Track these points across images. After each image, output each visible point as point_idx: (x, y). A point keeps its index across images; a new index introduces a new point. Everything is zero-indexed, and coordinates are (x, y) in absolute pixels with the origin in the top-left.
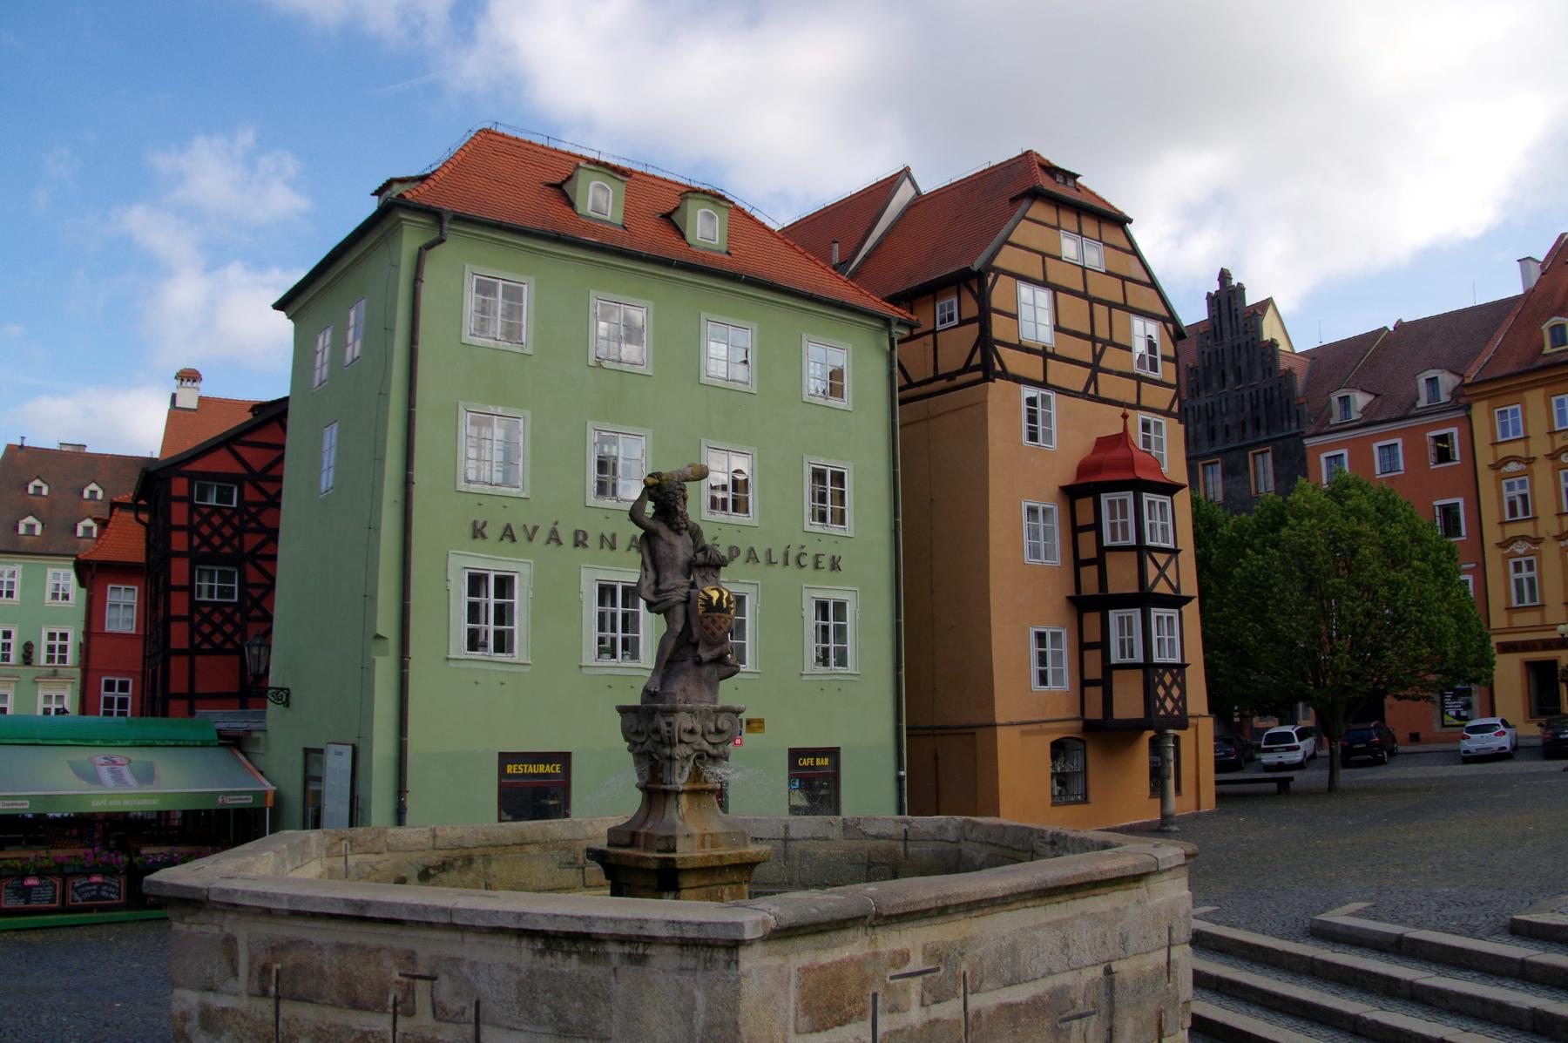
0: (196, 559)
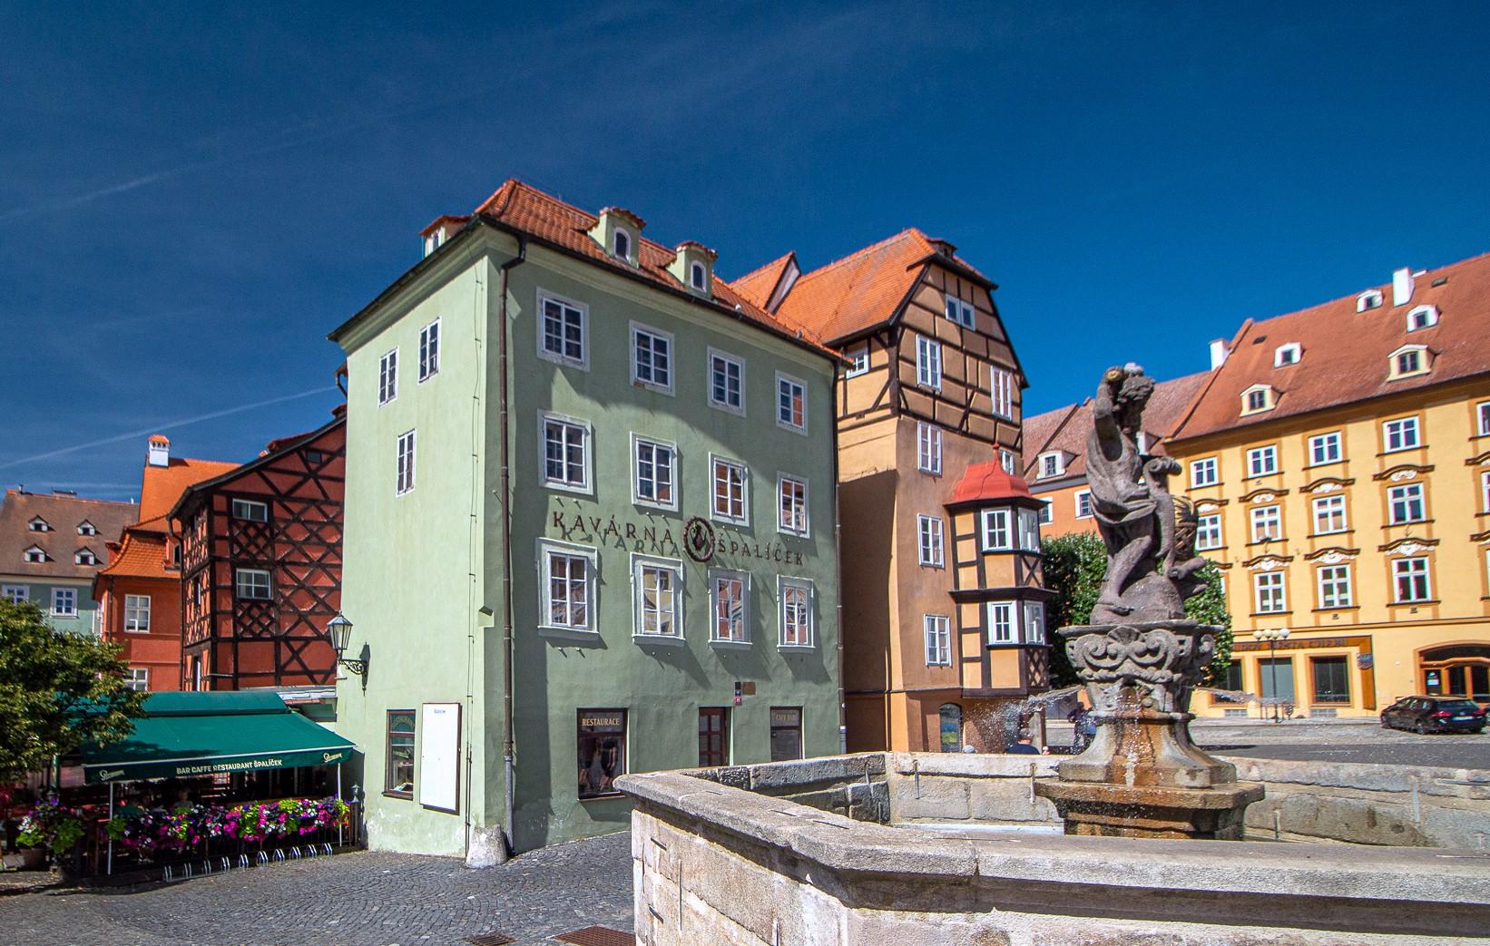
0: (236, 563)
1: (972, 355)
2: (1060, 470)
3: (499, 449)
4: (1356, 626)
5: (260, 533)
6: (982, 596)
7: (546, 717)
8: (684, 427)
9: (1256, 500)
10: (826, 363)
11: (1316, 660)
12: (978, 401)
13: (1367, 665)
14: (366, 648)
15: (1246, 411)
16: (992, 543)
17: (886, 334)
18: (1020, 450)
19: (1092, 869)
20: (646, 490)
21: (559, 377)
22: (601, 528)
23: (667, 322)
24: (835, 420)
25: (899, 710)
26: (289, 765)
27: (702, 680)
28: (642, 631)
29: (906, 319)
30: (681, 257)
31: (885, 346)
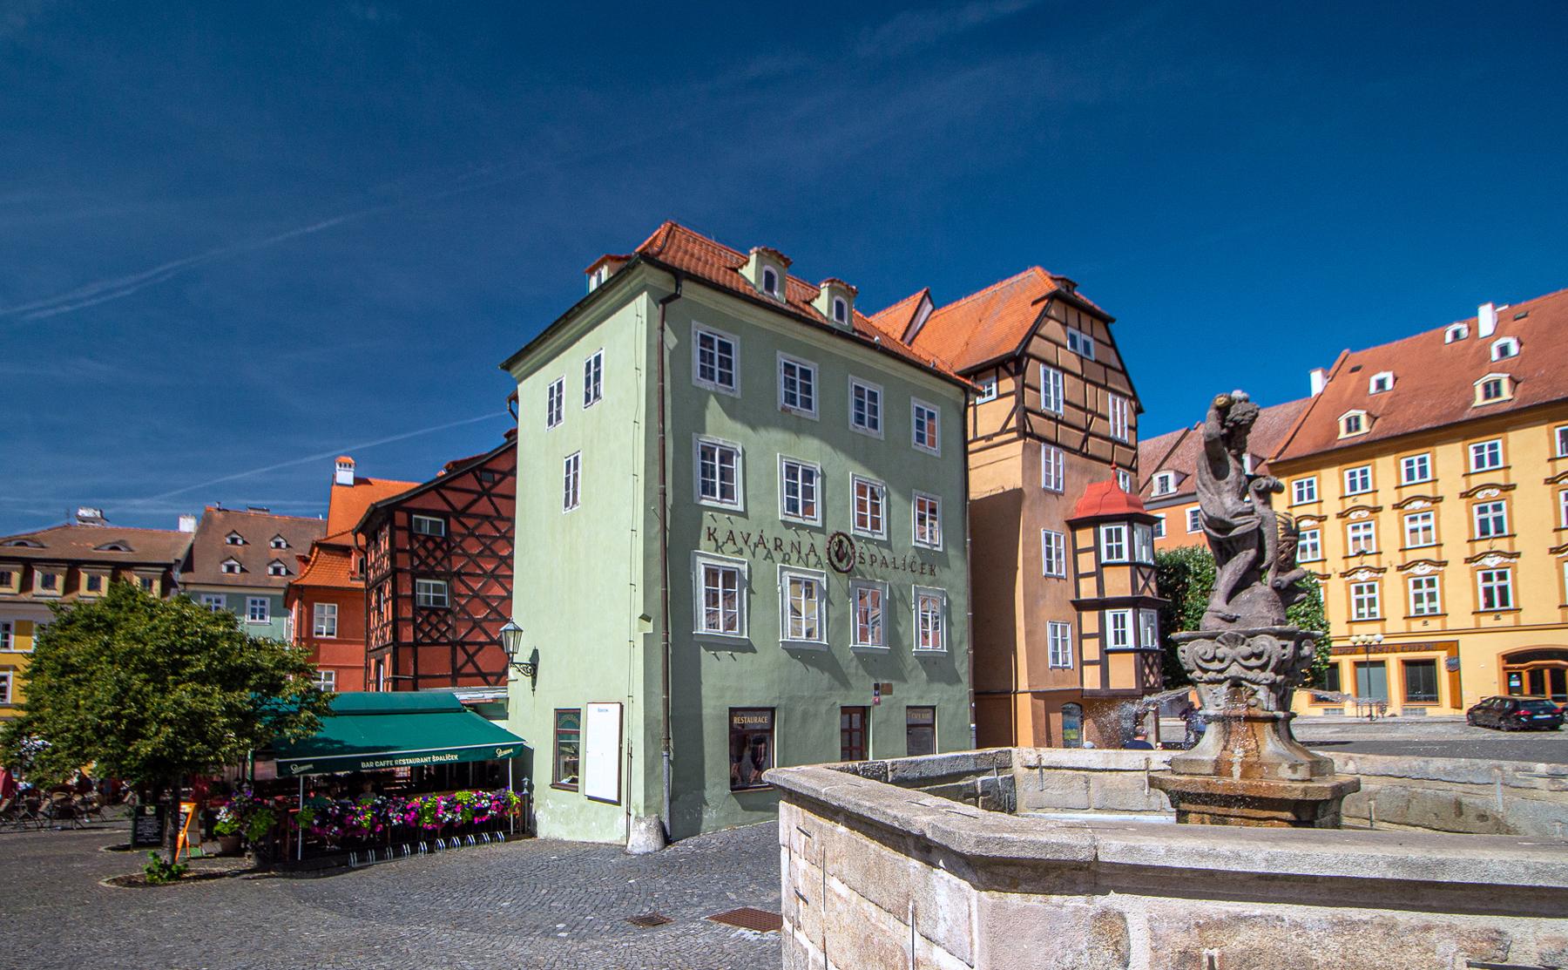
0: (415, 575)
1: (1092, 383)
2: (1172, 489)
3: (657, 469)
4: (1444, 632)
5: (438, 546)
6: (1100, 605)
7: (700, 716)
8: (828, 449)
9: (1353, 516)
10: (958, 390)
11: (1406, 663)
13: (1454, 668)
14: (535, 652)
15: (1343, 434)
16: (1110, 555)
17: (1013, 364)
18: (1136, 471)
19: (1202, 855)
20: (792, 506)
21: (713, 403)
22: (751, 543)
23: (812, 353)
24: (966, 443)
25: (1025, 707)
26: (464, 760)
27: (844, 681)
28: (789, 637)
29: (1031, 350)
30: (825, 292)
31: (1012, 375)
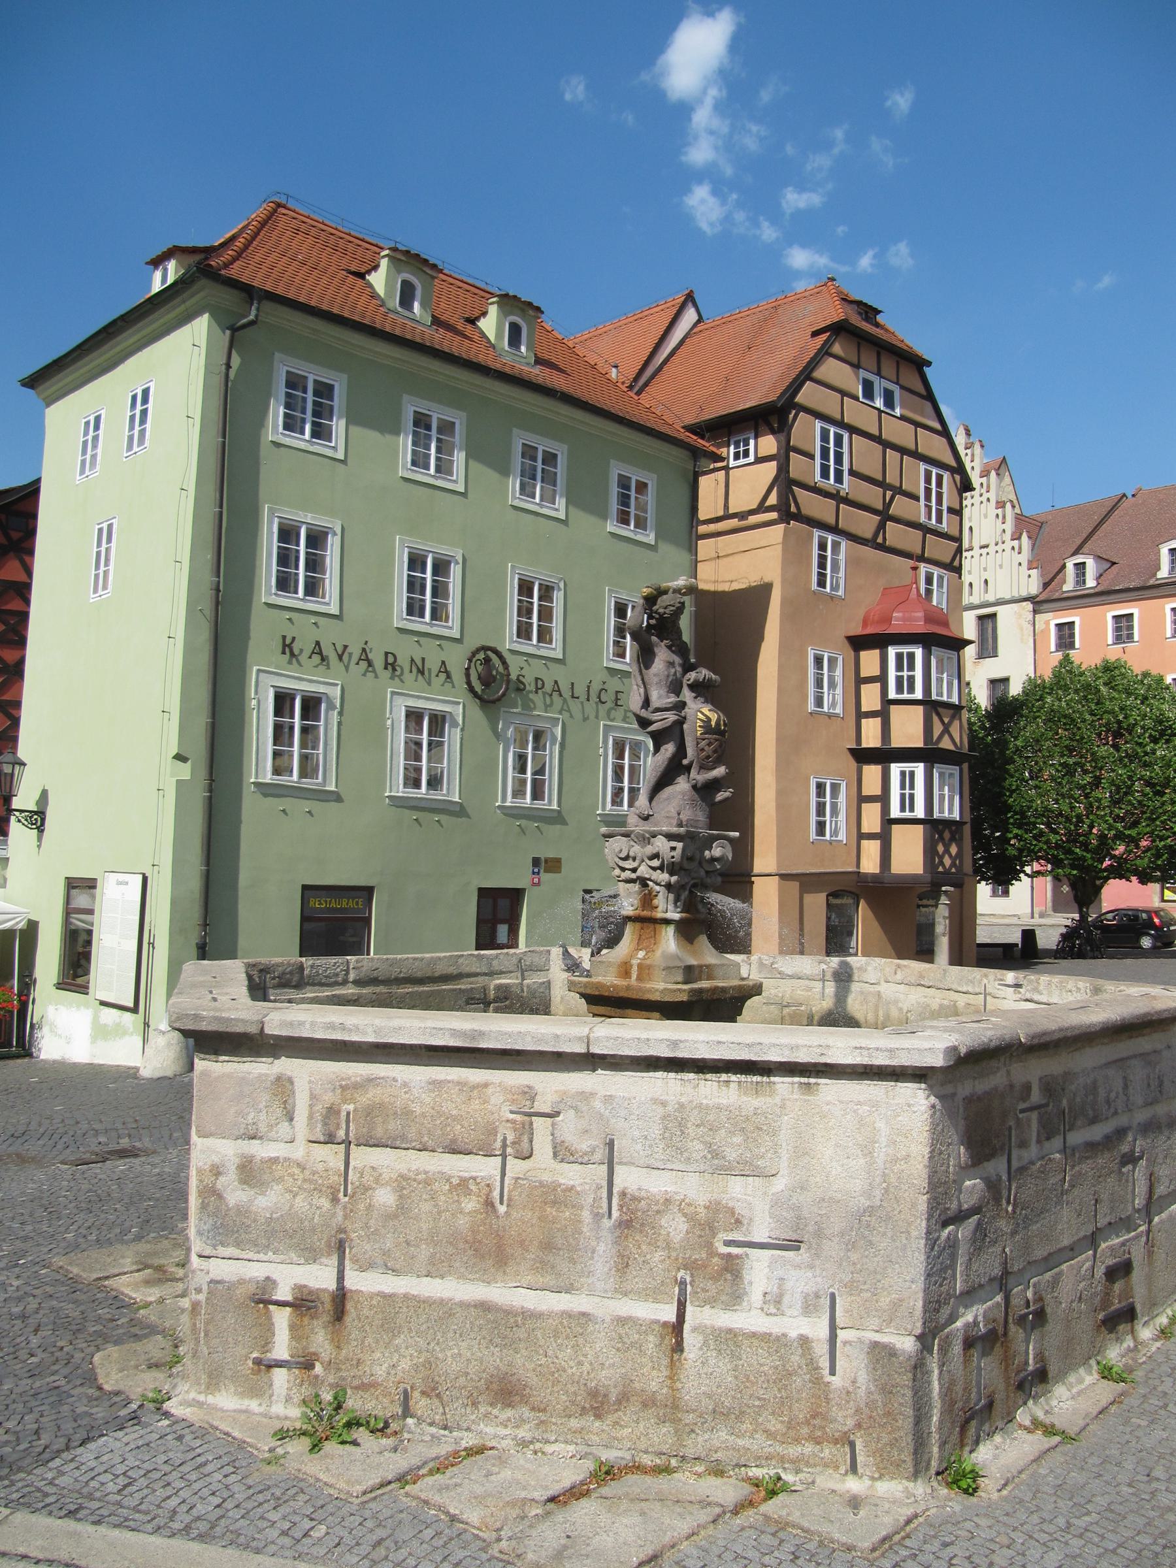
6: (884, 756)
12: (900, 506)
16: (900, 689)
31: (773, 432)
